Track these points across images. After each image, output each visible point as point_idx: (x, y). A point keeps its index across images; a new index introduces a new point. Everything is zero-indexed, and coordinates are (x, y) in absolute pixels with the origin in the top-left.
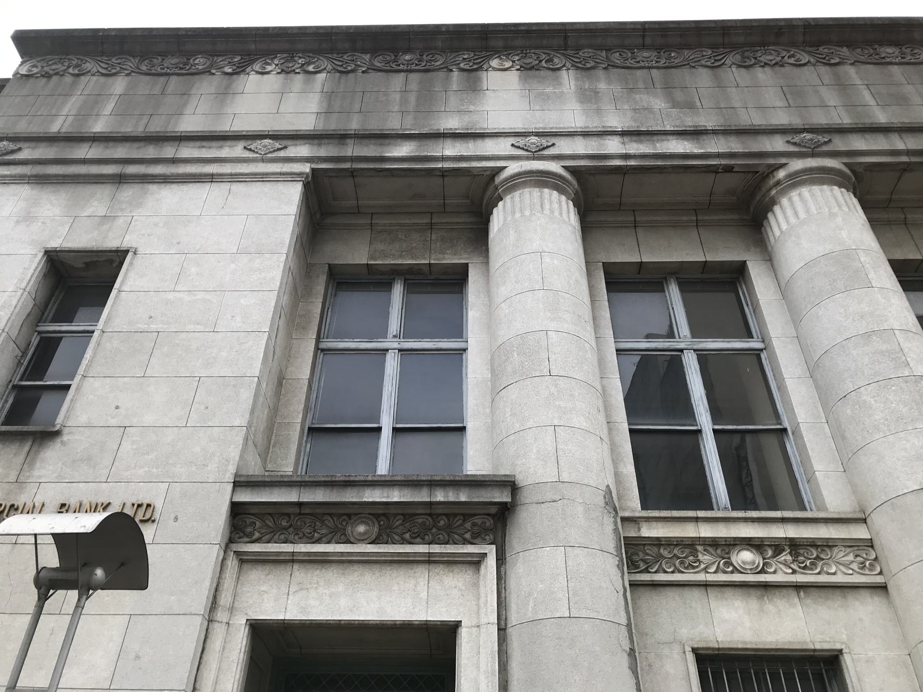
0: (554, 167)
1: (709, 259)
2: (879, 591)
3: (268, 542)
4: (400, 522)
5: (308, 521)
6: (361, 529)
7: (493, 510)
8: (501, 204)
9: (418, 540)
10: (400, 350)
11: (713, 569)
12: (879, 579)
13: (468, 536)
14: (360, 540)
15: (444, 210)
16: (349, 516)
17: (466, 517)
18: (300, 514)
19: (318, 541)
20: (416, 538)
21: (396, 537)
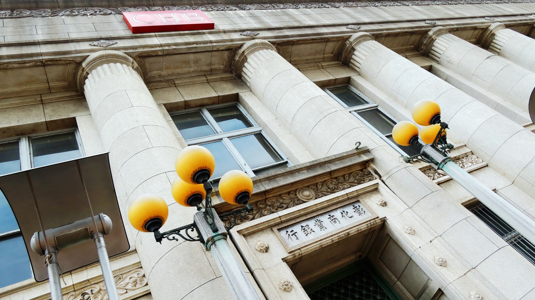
0: (266, 41)
1: (337, 77)
2: (486, 168)
3: (261, 217)
4: (320, 187)
5: (274, 200)
6: (307, 193)
7: (359, 168)
8: (249, 60)
9: (336, 190)
10: (228, 138)
11: (436, 177)
12: (484, 164)
13: (356, 181)
14: (309, 199)
15: (212, 72)
16: (295, 191)
17: (350, 174)
18: (266, 199)
19: (287, 208)
20: (334, 190)
21: (325, 193)
